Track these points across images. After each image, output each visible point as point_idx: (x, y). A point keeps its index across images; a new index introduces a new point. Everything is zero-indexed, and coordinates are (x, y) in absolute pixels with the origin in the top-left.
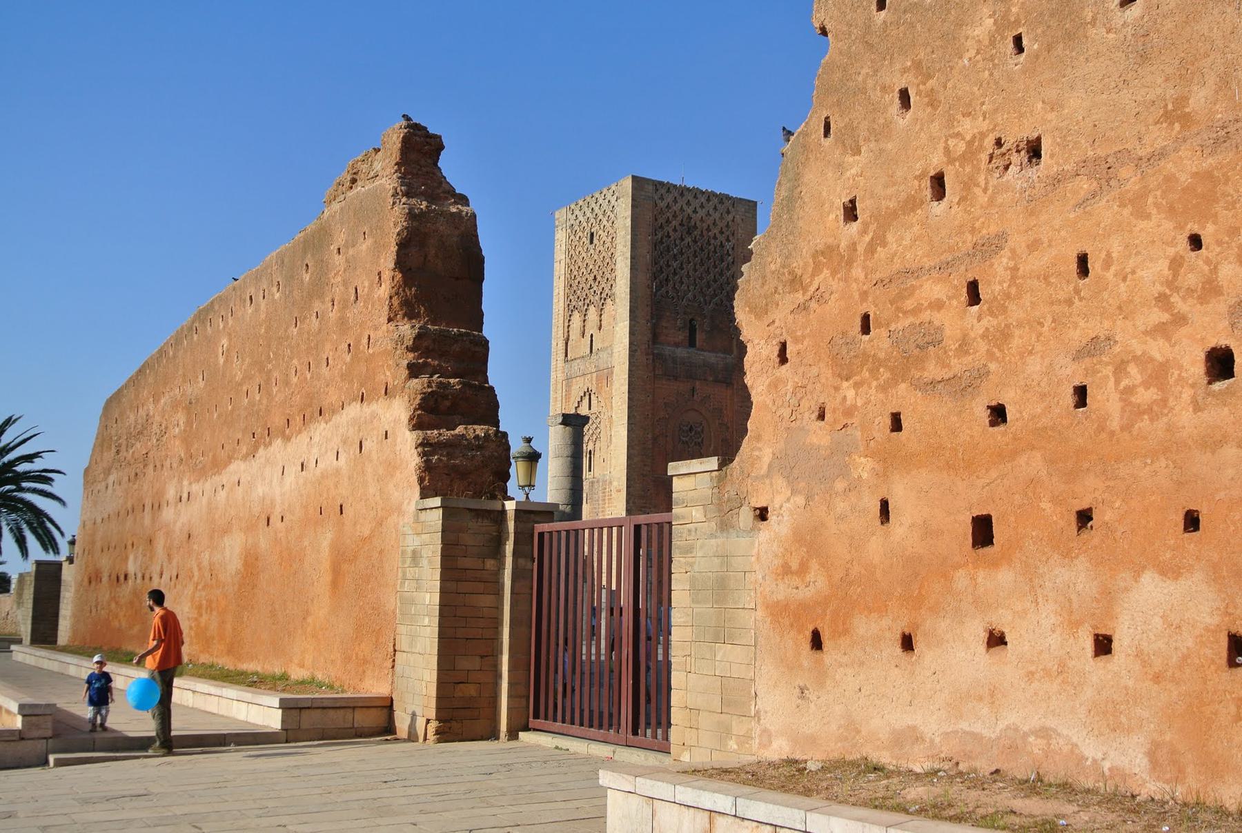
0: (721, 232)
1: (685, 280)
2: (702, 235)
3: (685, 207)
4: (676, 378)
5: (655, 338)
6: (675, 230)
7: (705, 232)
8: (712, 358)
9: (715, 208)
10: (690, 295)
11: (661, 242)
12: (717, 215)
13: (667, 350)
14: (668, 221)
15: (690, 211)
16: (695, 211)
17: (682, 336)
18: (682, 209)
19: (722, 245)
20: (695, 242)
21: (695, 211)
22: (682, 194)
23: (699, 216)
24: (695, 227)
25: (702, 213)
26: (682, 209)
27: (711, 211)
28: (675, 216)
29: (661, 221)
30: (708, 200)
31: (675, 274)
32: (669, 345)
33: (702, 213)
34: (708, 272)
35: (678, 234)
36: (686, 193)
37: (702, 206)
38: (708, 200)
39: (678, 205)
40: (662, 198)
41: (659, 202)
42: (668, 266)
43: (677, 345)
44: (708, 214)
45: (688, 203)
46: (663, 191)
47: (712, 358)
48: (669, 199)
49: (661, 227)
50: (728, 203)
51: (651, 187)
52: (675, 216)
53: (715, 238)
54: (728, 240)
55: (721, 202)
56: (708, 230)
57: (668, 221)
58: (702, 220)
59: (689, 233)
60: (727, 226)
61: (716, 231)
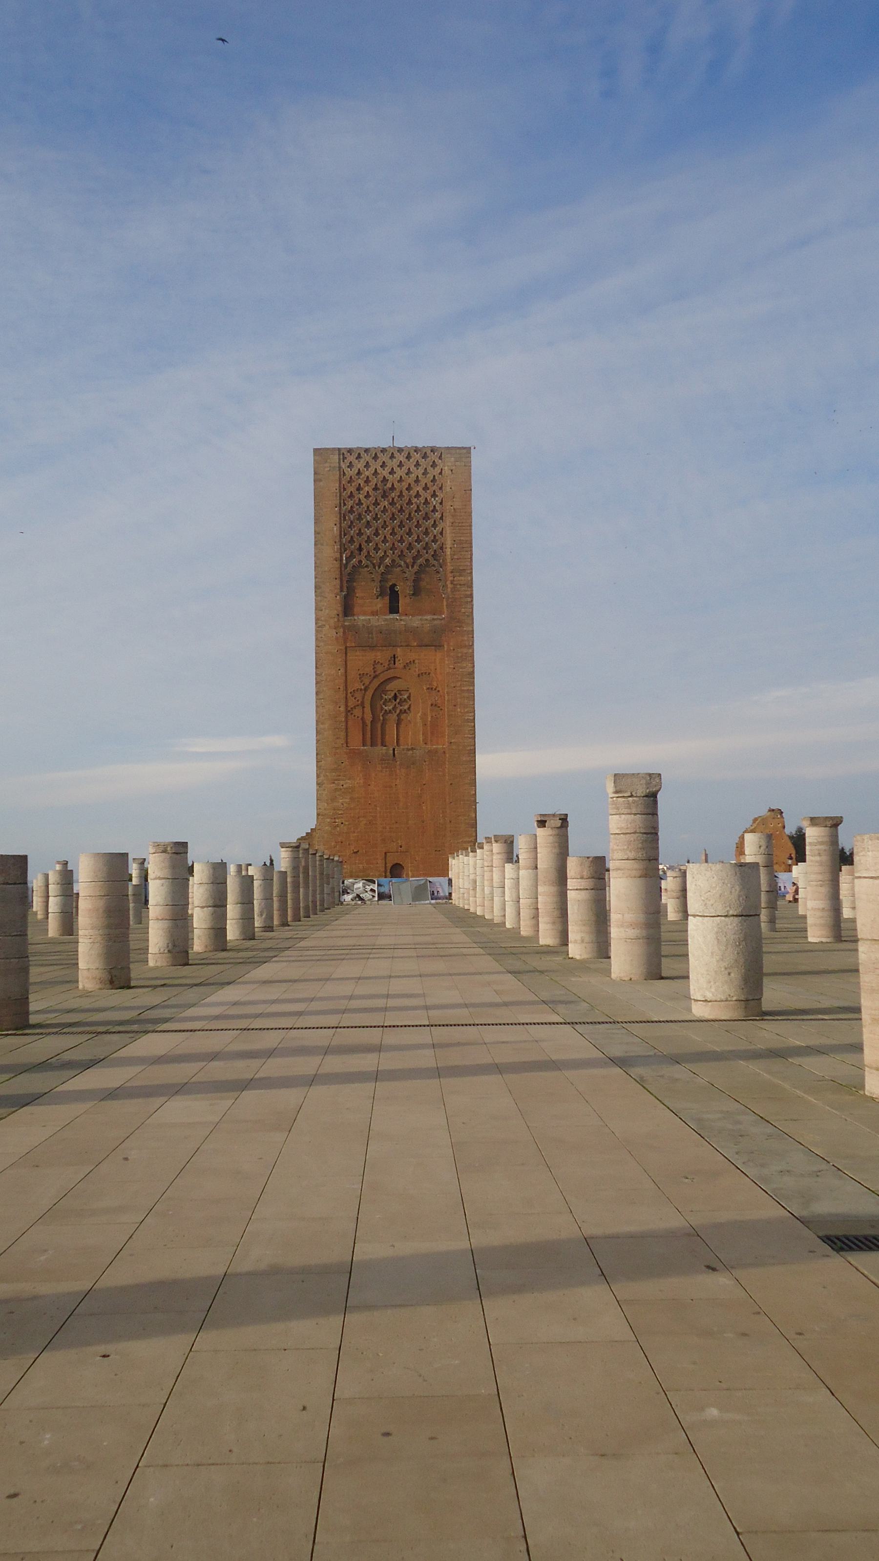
0: (426, 488)
1: (382, 546)
2: (401, 495)
3: (380, 470)
4: (372, 647)
5: (347, 609)
6: (367, 496)
7: (405, 493)
8: (415, 622)
9: (417, 465)
10: (388, 561)
11: (351, 511)
12: (421, 470)
13: (361, 619)
14: (359, 489)
15: (385, 473)
16: (392, 472)
17: (382, 603)
18: (376, 473)
19: (426, 502)
20: (392, 503)
21: (392, 472)
22: (375, 458)
23: (397, 476)
24: (393, 488)
25: (399, 472)
26: (376, 473)
27: (412, 468)
28: (367, 481)
29: (352, 488)
30: (408, 457)
31: (368, 541)
32: (365, 614)
33: (399, 472)
34: (409, 533)
35: (372, 499)
36: (380, 455)
37: (401, 465)
38: (408, 457)
39: (372, 470)
40: (351, 466)
41: (347, 470)
42: (360, 534)
43: (374, 613)
44: (409, 472)
45: (383, 465)
46: (352, 458)
47: (415, 622)
48: (360, 465)
49: (351, 496)
50: (433, 457)
51: (336, 457)
52: (367, 481)
53: (418, 495)
54: (434, 495)
55: (425, 456)
56: (409, 488)
57: (359, 489)
58: (401, 480)
59: (384, 496)
60: (434, 480)
61: (420, 489)
